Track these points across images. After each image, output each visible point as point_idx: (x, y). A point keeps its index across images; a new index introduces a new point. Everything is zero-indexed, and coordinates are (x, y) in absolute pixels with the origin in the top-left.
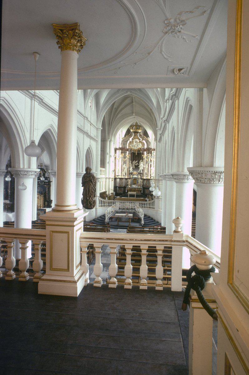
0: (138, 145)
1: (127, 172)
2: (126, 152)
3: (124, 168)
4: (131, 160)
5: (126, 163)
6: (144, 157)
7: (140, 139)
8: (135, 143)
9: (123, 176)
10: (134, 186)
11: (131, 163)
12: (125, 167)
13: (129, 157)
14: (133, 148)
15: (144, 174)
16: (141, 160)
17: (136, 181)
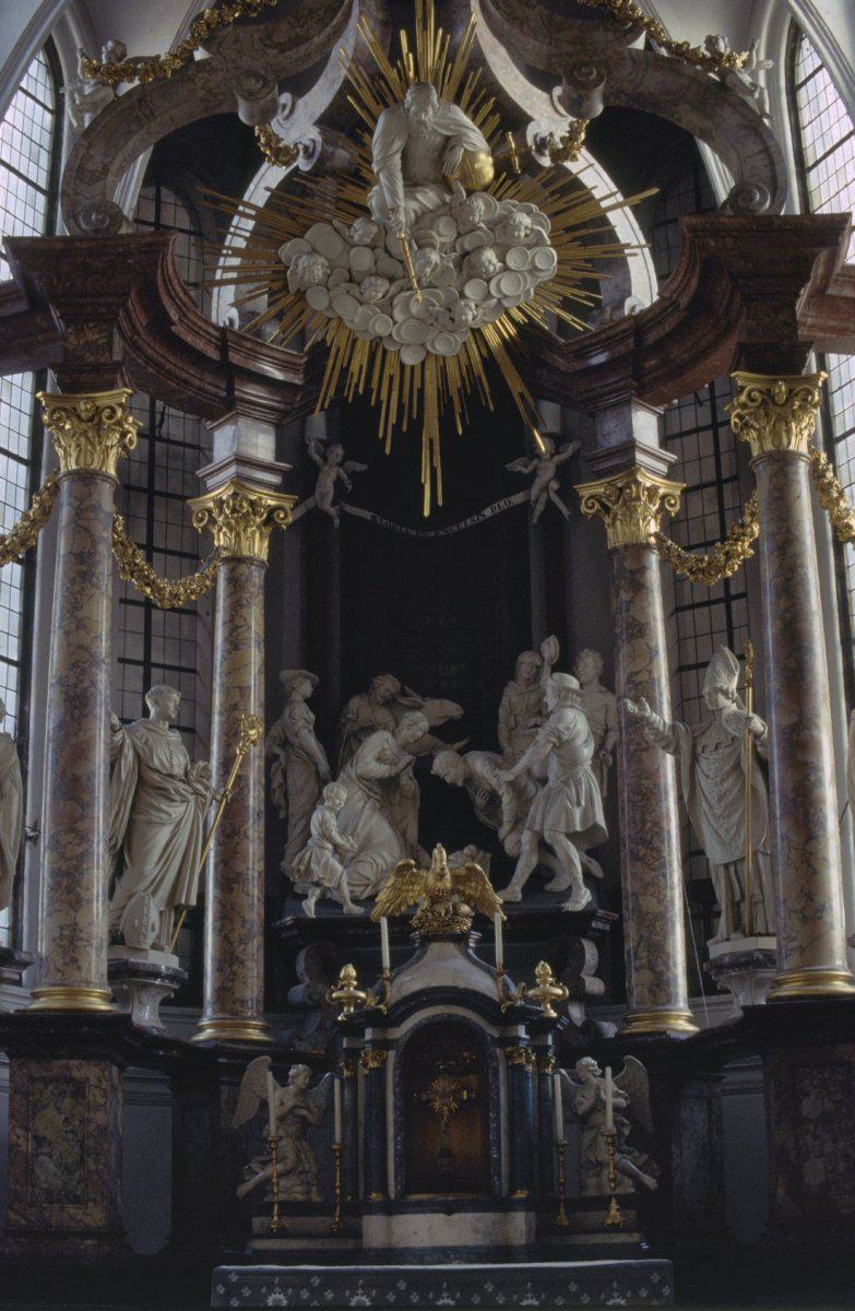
0: (466, 263)
1: (227, 914)
2: (203, 451)
3: (146, 787)
4: (311, 660)
5: (190, 674)
6: (617, 535)
7: (510, 119)
8: (412, 184)
9: (96, 962)
10: (423, 1229)
11: (301, 717)
12: (171, 754)
13: (259, 548)
14: (361, 317)
15: (655, 924)
16: (551, 648)
17: (477, 1107)
